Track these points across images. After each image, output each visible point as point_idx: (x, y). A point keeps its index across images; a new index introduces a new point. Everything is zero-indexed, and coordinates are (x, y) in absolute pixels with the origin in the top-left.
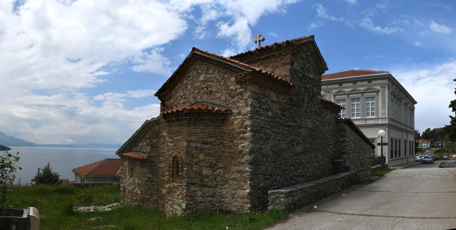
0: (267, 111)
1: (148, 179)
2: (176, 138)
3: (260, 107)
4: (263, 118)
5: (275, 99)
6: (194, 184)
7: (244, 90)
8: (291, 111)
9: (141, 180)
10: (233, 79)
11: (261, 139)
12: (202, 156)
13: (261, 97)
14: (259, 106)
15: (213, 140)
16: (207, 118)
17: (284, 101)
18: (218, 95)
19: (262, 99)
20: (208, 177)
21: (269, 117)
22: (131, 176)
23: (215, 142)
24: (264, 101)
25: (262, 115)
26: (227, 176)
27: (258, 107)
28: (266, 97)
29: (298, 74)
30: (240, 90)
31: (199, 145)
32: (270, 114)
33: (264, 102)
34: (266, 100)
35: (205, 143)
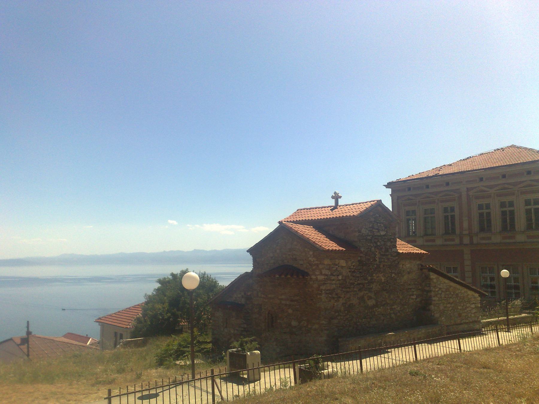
0: (338, 275)
1: (243, 329)
2: (270, 296)
3: (332, 274)
4: (334, 282)
5: (344, 265)
6: (285, 333)
7: (319, 262)
8: (361, 271)
9: (237, 330)
10: (311, 253)
11: (334, 298)
12: (290, 311)
13: (332, 266)
14: (331, 274)
15: (298, 298)
16: (293, 281)
17: (354, 264)
18: (301, 262)
19: (333, 268)
20: (295, 327)
21: (339, 280)
22: (226, 327)
23: (299, 300)
24: (335, 269)
25: (333, 280)
26: (309, 326)
27: (330, 275)
28: (336, 265)
29: (366, 237)
30: (317, 262)
31: (288, 303)
32: (340, 277)
33: (335, 270)
34: (337, 268)
35: (292, 301)
